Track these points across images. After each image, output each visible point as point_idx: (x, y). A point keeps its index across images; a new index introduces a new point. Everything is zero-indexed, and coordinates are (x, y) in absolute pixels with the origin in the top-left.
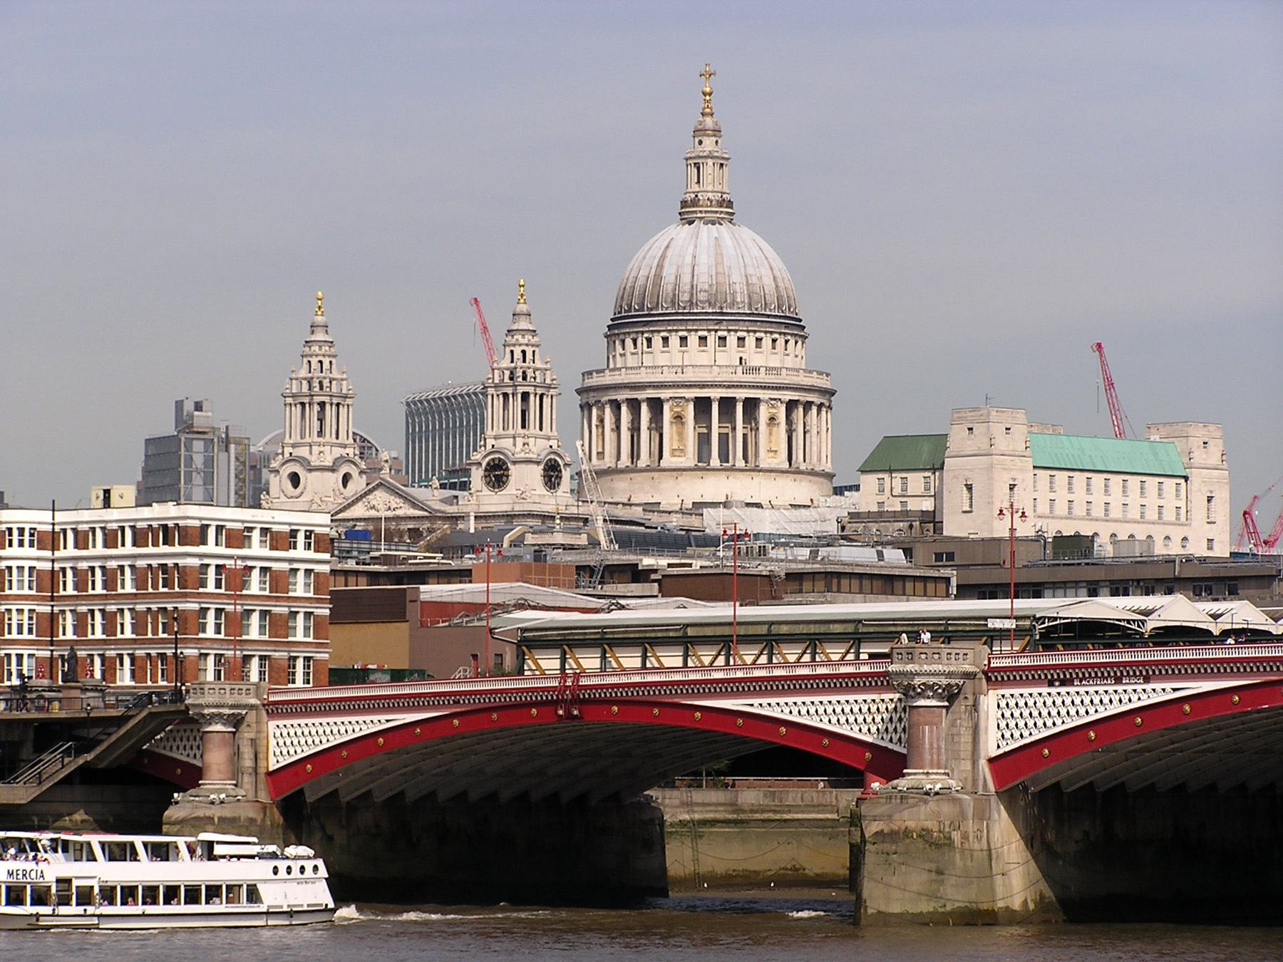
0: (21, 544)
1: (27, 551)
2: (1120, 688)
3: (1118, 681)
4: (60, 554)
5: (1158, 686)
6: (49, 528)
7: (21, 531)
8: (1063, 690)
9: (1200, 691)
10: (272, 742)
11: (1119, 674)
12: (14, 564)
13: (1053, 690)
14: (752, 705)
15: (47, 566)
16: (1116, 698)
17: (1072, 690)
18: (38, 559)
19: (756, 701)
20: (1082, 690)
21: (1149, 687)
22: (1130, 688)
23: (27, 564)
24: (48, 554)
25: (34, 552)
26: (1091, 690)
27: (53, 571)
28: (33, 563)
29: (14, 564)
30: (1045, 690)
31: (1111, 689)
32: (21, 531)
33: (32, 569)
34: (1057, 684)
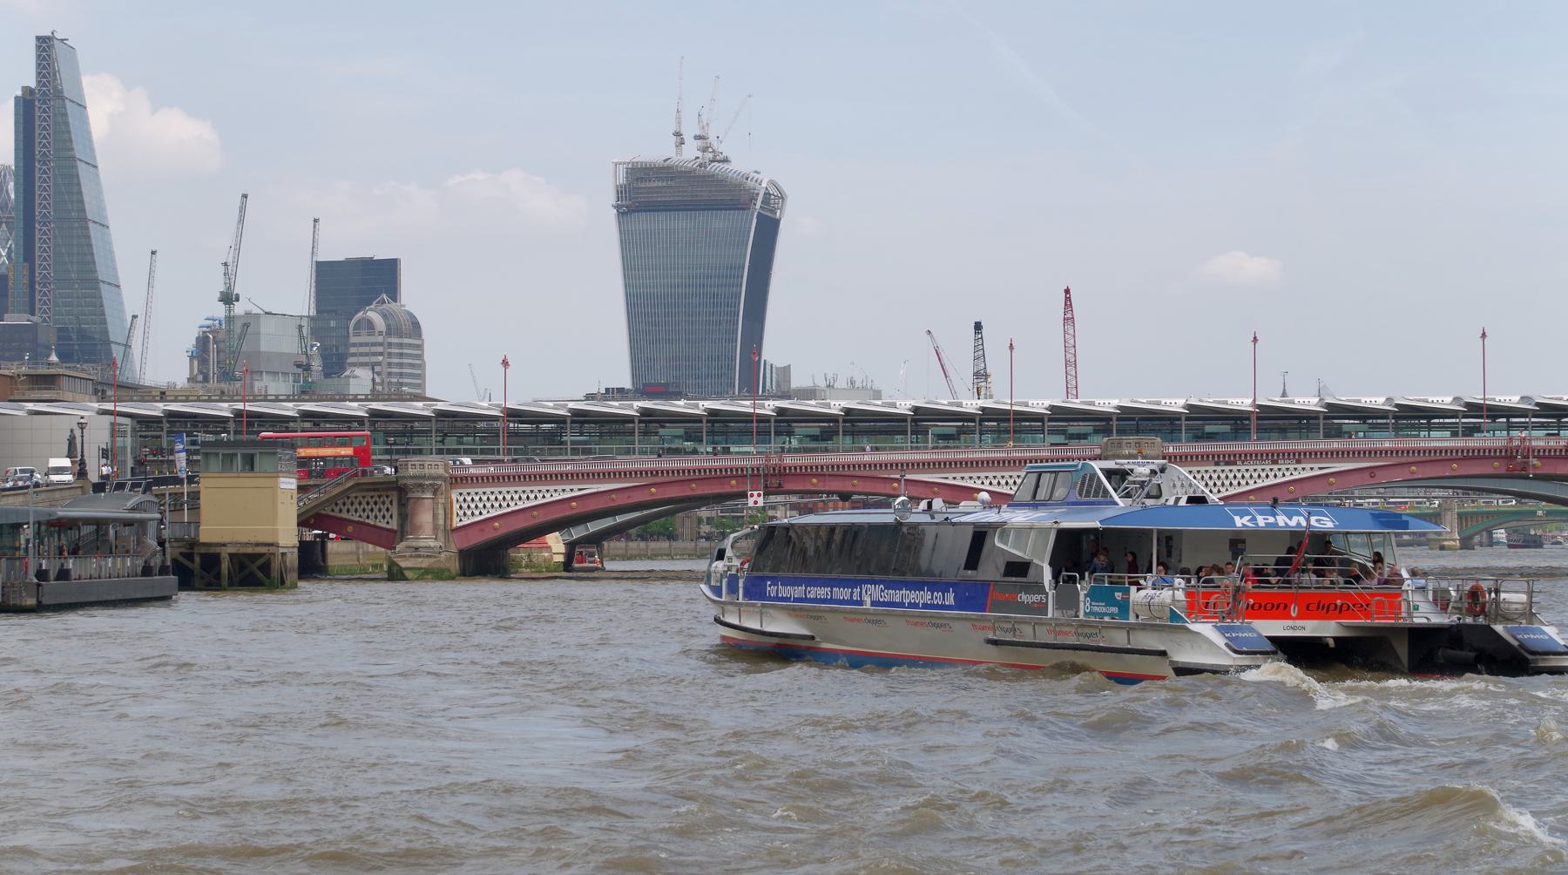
2: (1275, 467)
3: (1275, 462)
5: (1307, 466)
8: (1227, 468)
9: (1342, 469)
10: (456, 506)
11: (1275, 458)
13: (1219, 469)
14: (947, 478)
16: (1271, 474)
17: (1235, 468)
19: (951, 476)
20: (1243, 468)
21: (1299, 466)
22: (1283, 467)
26: (1251, 468)
30: (1211, 469)
31: (1267, 468)
34: (1222, 464)
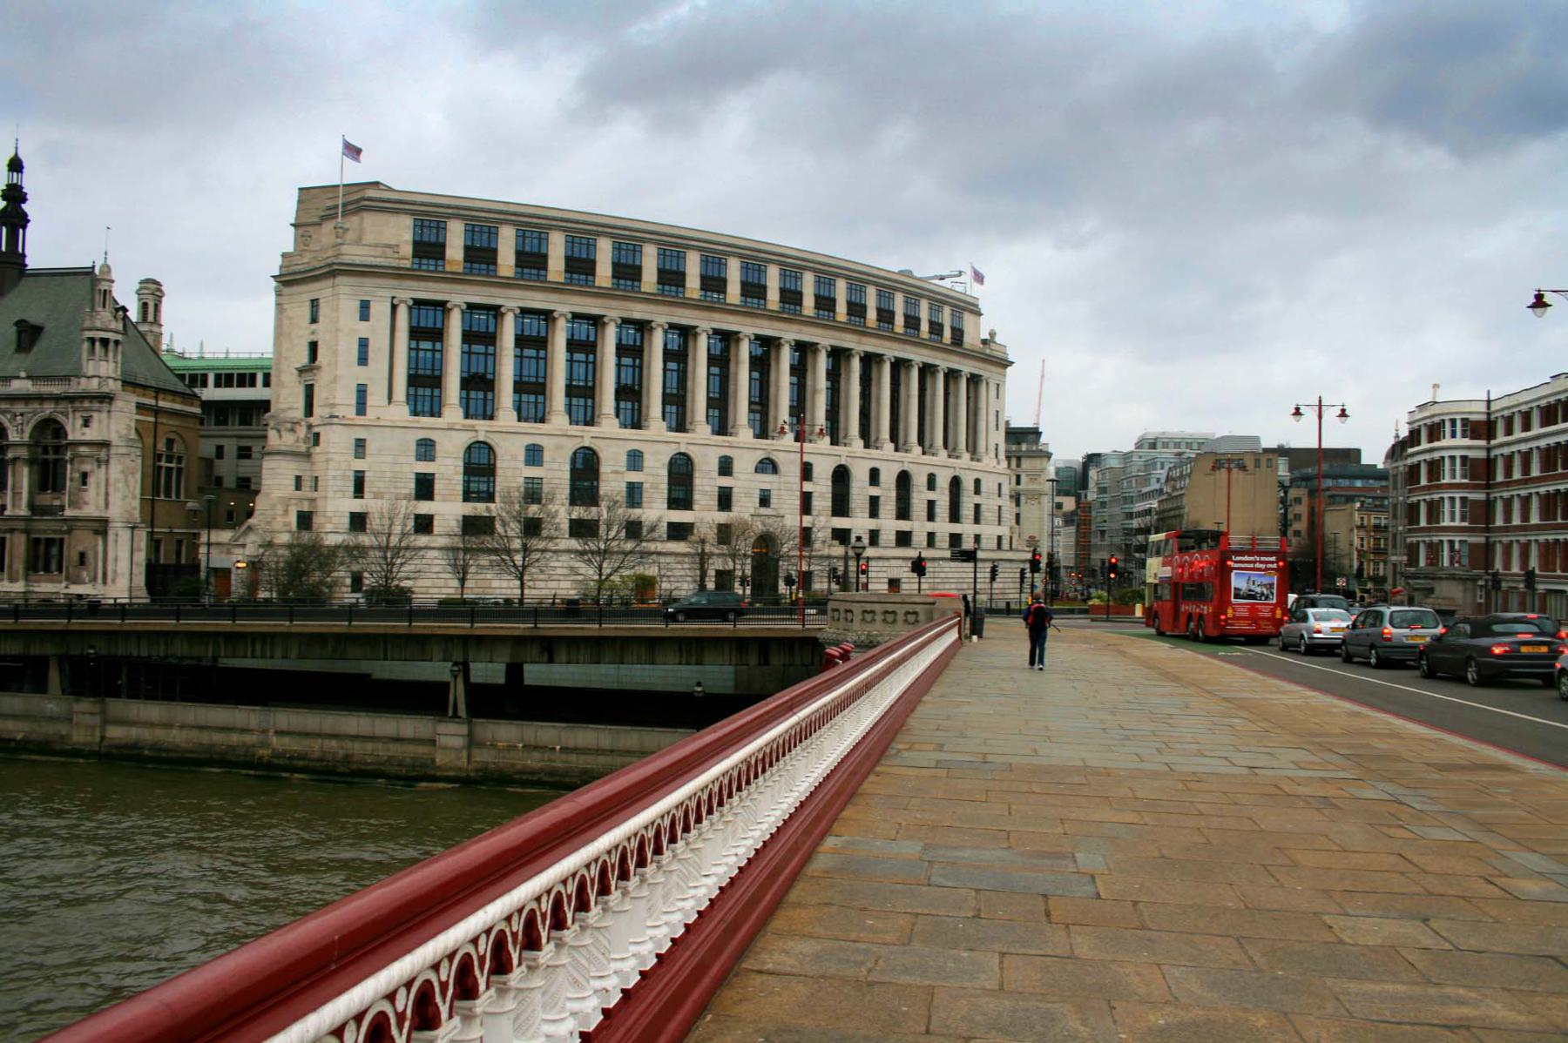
0: (1453, 435)
1: (1460, 441)
4: (1493, 442)
6: (1483, 418)
7: (1453, 422)
12: (1446, 454)
15: (1482, 454)
18: (1469, 448)
23: (1457, 453)
24: (1482, 443)
25: (1467, 442)
27: (1489, 463)
28: (1464, 453)
29: (1446, 454)
32: (1453, 422)
33: (1464, 458)
